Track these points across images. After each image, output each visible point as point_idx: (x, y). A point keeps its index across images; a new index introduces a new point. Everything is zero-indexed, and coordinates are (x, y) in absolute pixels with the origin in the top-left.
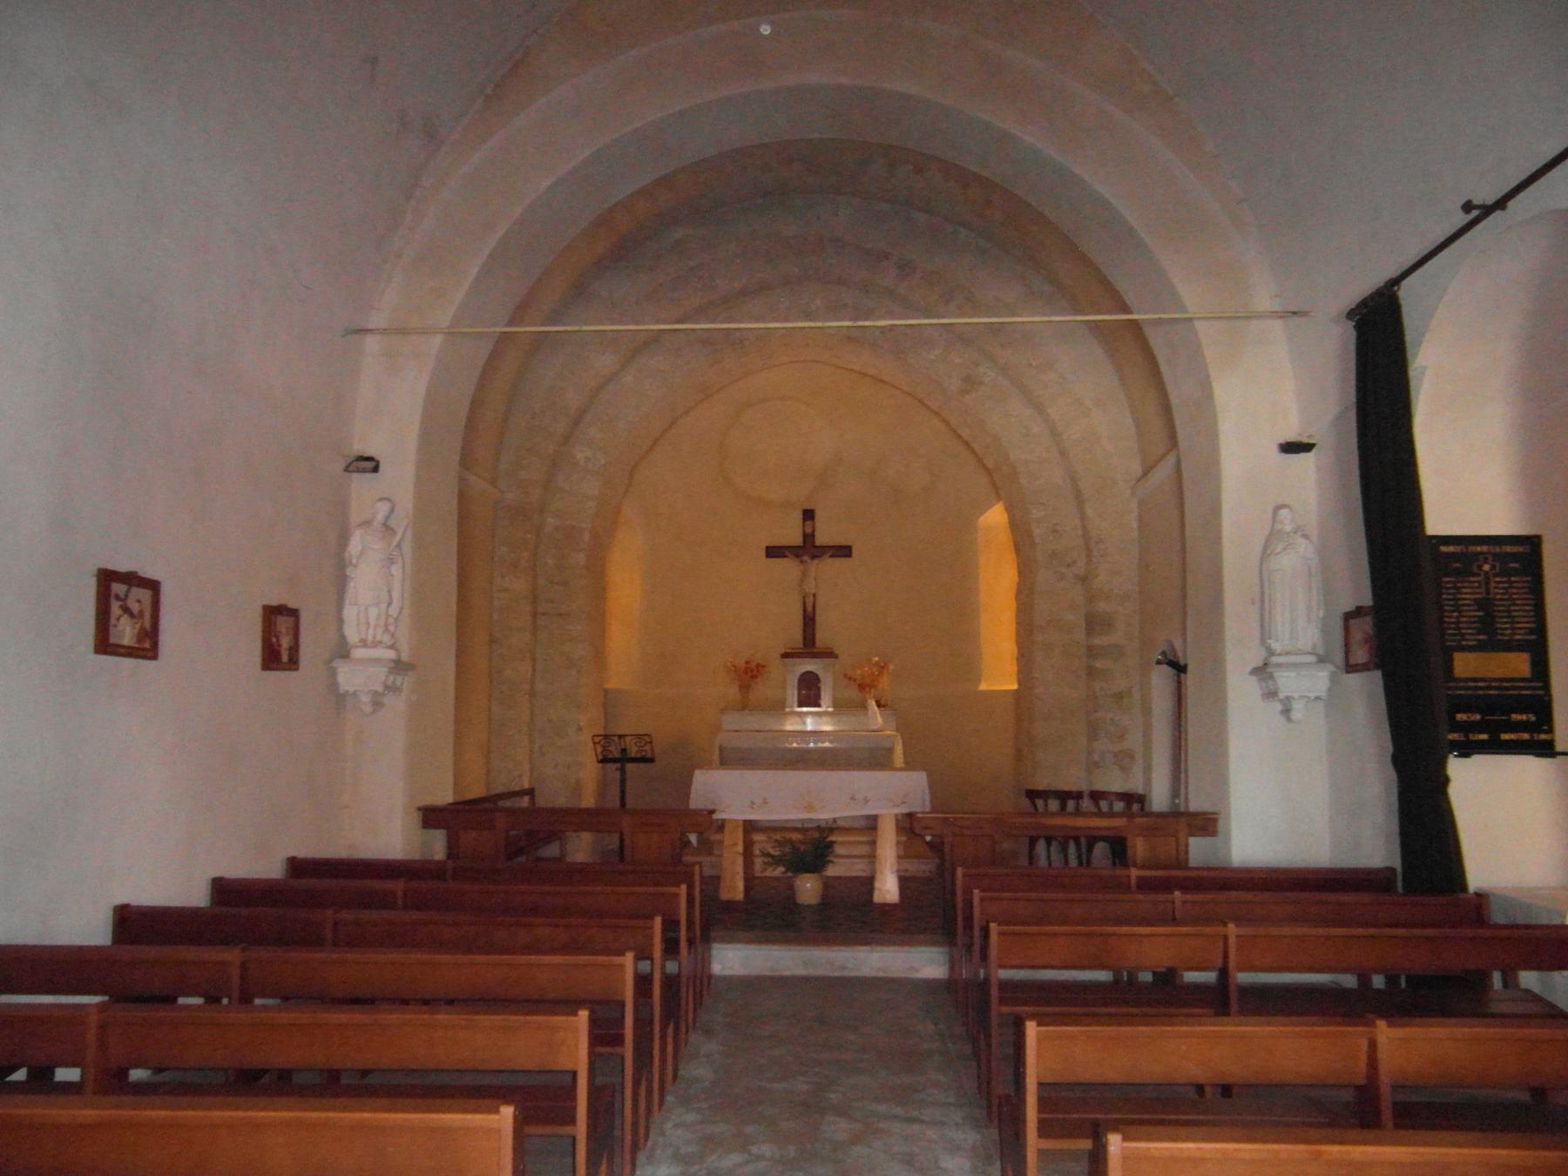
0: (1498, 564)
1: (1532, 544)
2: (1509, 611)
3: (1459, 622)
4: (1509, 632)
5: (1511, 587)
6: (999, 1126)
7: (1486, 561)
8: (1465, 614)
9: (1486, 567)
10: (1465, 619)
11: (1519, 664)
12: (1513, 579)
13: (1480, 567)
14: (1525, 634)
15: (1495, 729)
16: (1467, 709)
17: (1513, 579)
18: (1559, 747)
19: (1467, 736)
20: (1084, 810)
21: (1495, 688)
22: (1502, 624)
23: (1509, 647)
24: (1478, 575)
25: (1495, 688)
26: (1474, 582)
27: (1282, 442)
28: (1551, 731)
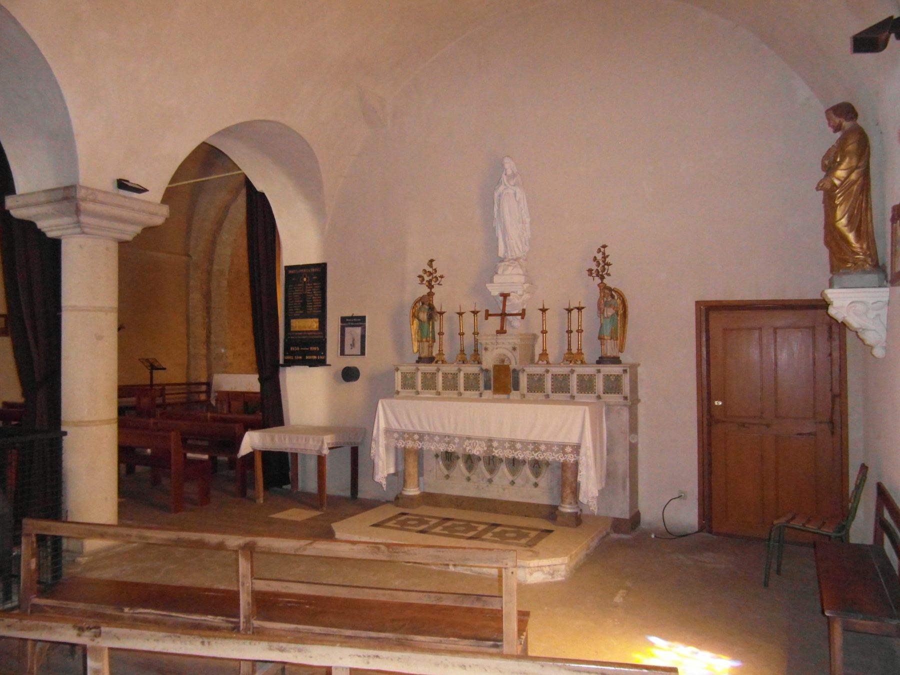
0: (309, 278)
1: (321, 269)
2: (312, 299)
3: (313, 308)
4: (311, 309)
5: (313, 288)
6: (536, 536)
7: (305, 277)
8: (296, 301)
9: (305, 279)
10: (316, 306)
11: (312, 324)
12: (314, 284)
13: (302, 280)
14: (317, 310)
15: (304, 354)
16: (296, 345)
17: (314, 284)
18: (328, 363)
19: (294, 358)
20: (162, 402)
21: (305, 335)
22: (309, 306)
23: (311, 316)
24: (301, 283)
25: (305, 335)
26: (299, 287)
27: (118, 178)
28: (325, 355)
